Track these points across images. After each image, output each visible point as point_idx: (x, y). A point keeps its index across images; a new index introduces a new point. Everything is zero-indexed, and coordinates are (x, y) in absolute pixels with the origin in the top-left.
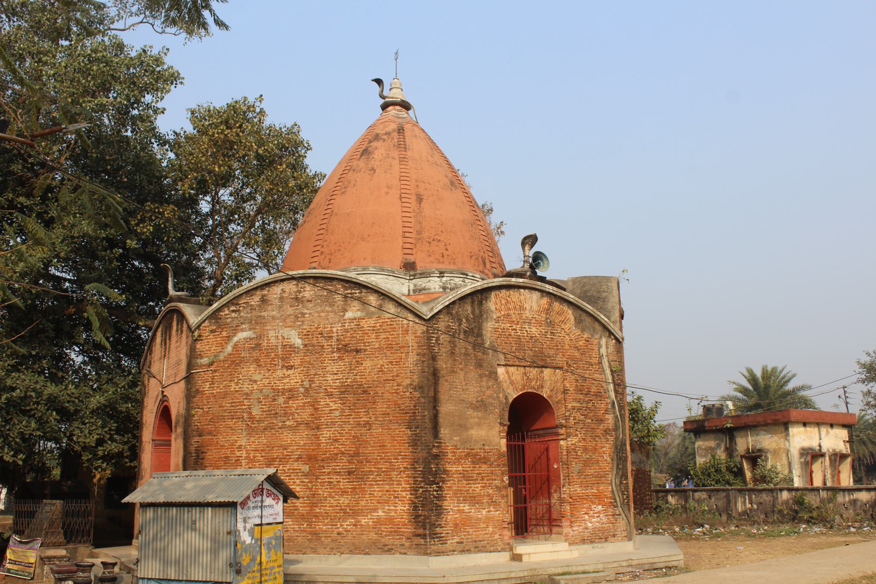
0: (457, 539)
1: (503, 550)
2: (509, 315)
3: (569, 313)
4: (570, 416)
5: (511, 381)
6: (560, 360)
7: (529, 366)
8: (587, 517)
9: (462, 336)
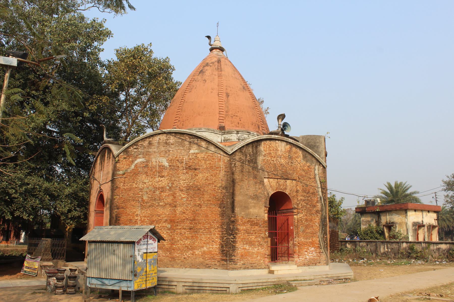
0: (242, 262)
1: (265, 268)
2: (270, 153)
3: (300, 153)
4: (299, 203)
5: (271, 186)
6: (295, 176)
7: (280, 179)
8: (306, 253)
9: (247, 163)
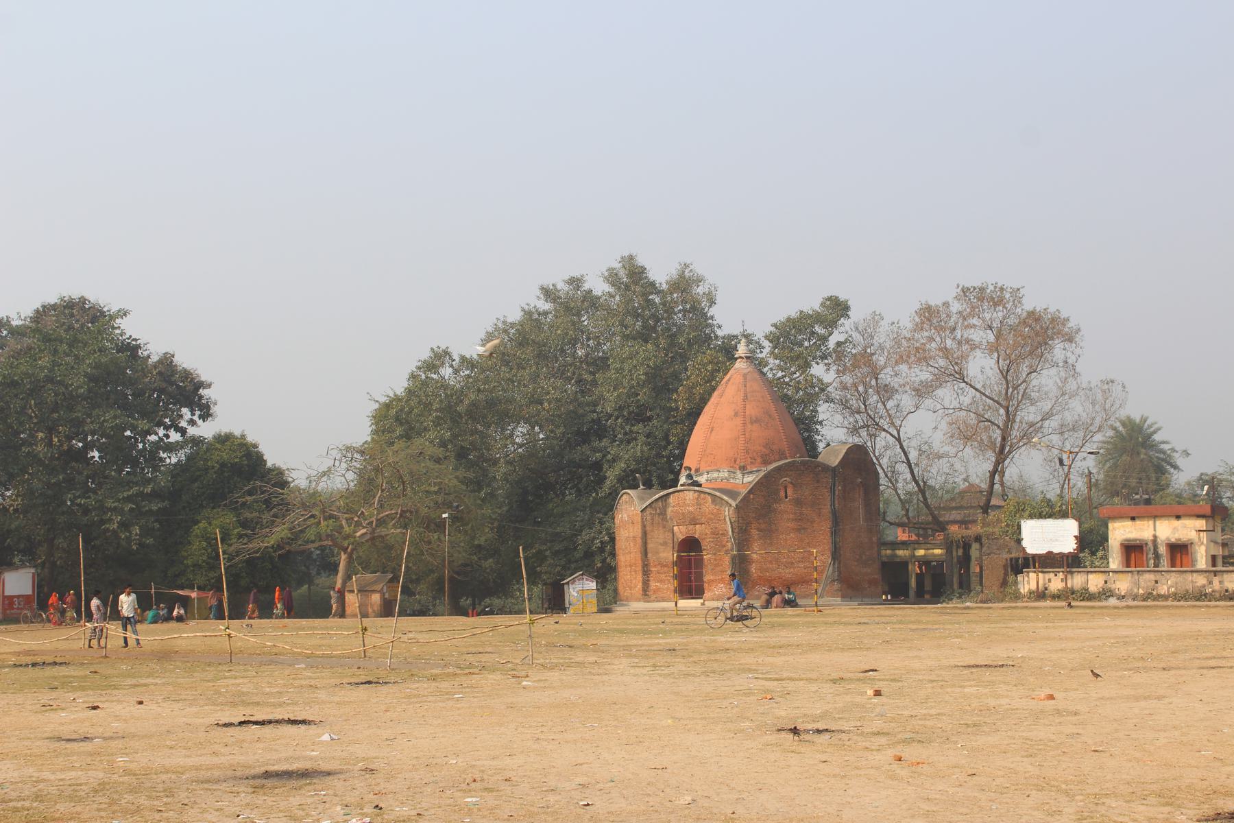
3: (709, 499)
5: (681, 532)
6: (703, 520)
